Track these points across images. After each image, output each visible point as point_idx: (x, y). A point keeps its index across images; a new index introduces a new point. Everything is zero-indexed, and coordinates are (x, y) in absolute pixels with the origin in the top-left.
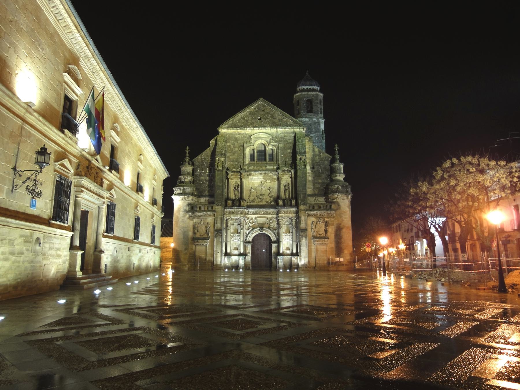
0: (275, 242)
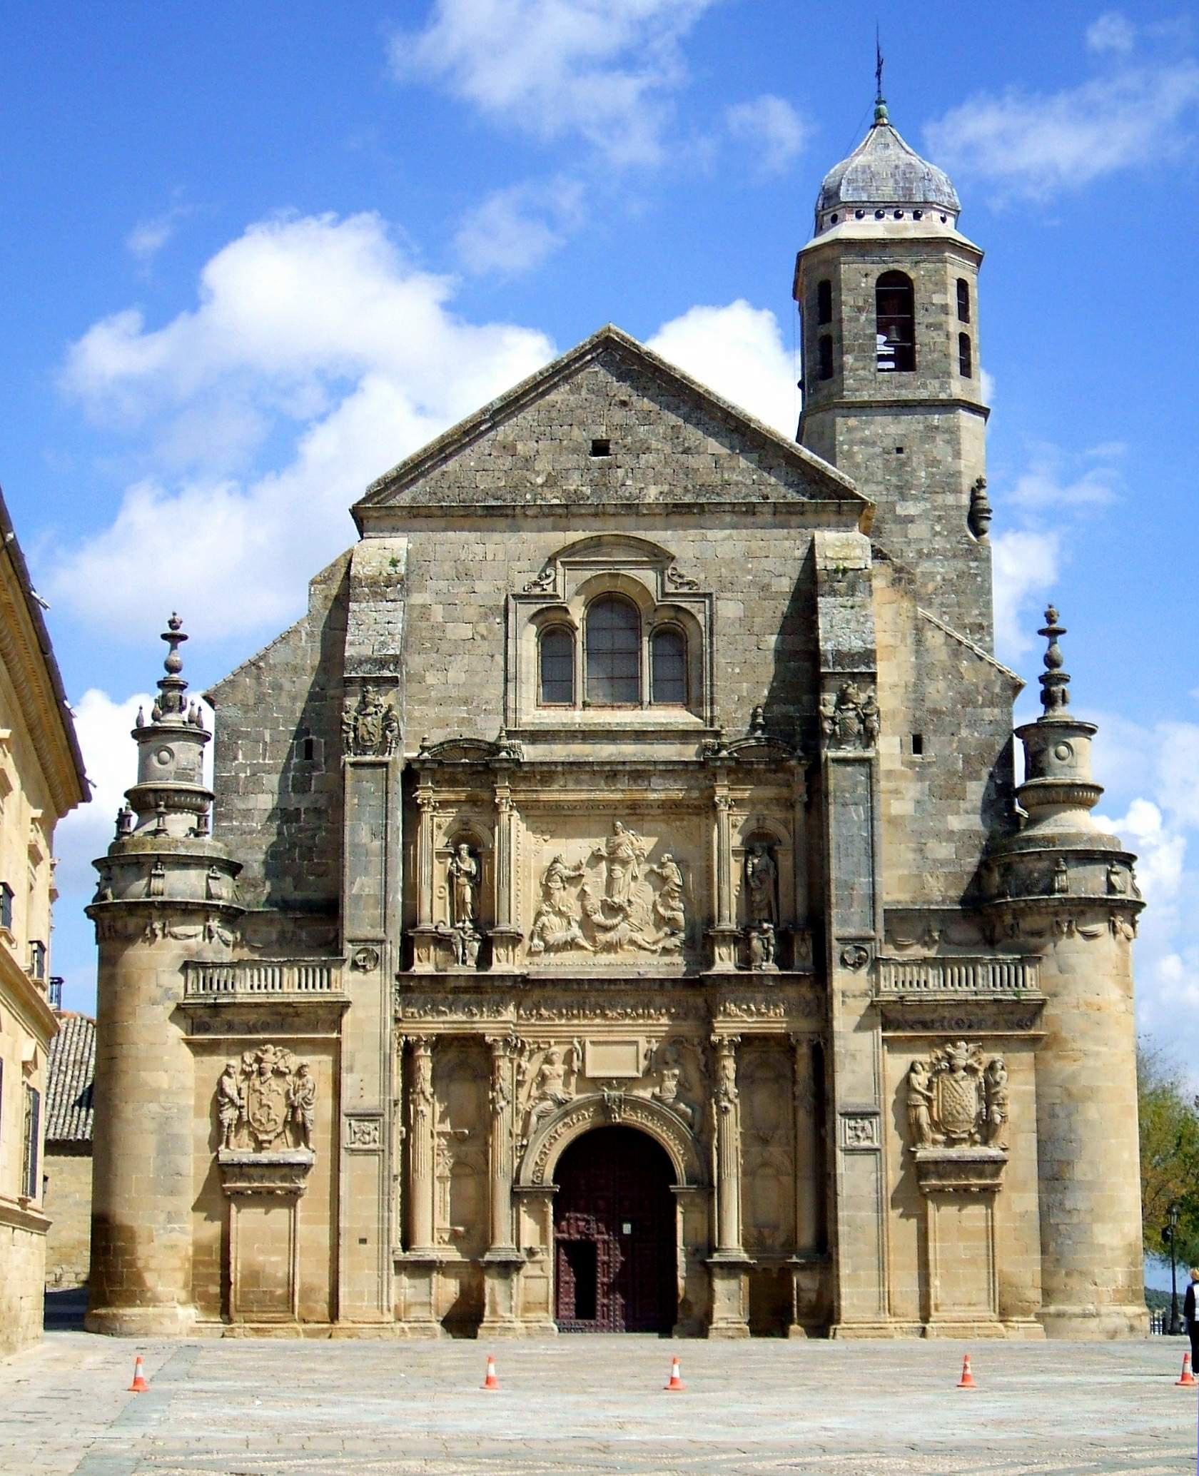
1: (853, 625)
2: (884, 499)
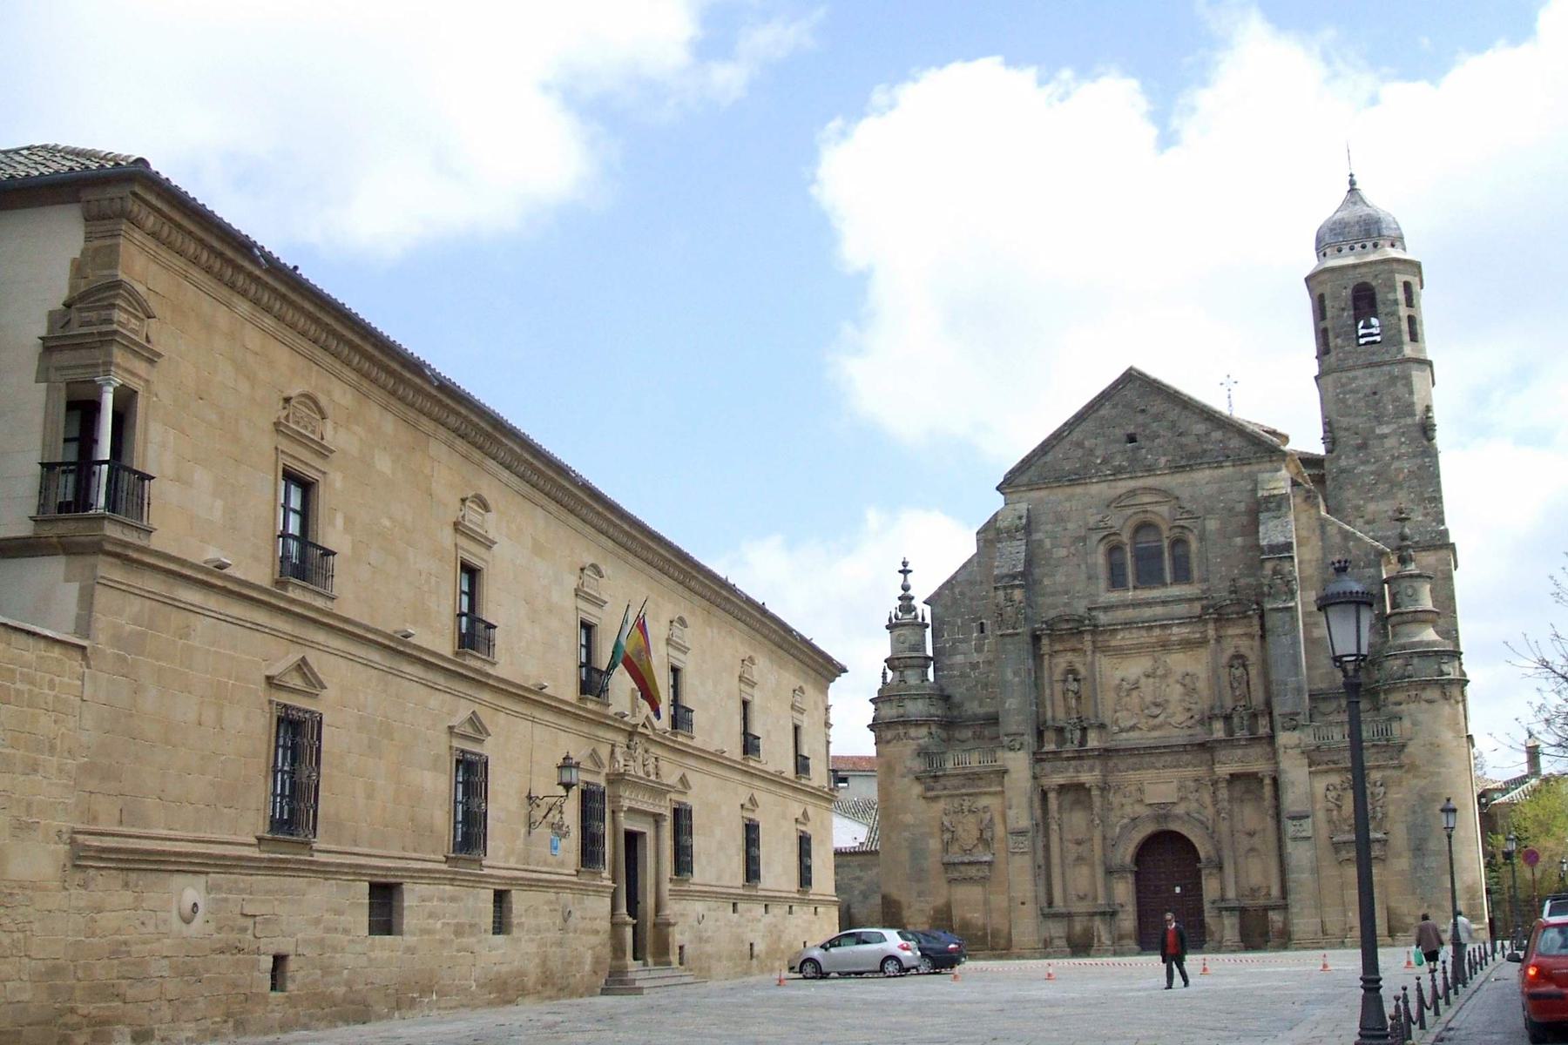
0: (1209, 860)
1: (1279, 528)
2: (1368, 425)
